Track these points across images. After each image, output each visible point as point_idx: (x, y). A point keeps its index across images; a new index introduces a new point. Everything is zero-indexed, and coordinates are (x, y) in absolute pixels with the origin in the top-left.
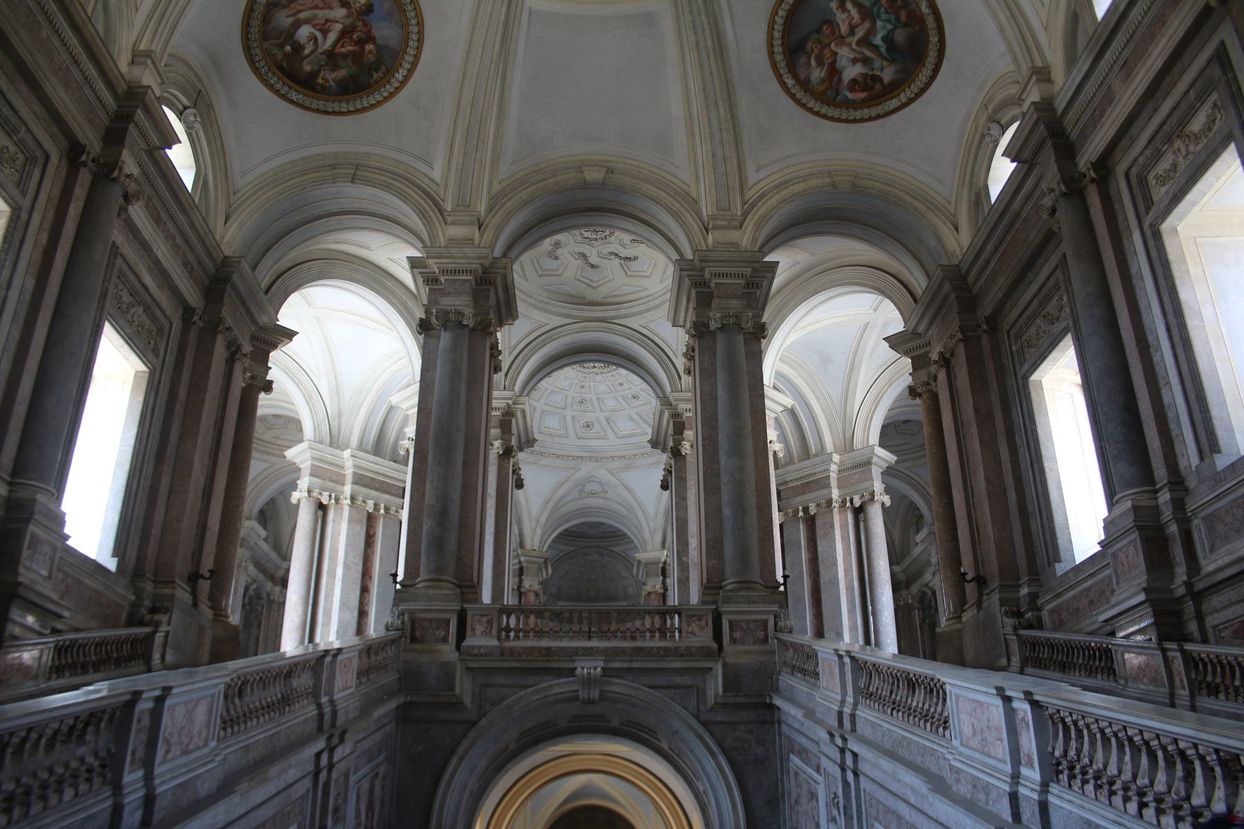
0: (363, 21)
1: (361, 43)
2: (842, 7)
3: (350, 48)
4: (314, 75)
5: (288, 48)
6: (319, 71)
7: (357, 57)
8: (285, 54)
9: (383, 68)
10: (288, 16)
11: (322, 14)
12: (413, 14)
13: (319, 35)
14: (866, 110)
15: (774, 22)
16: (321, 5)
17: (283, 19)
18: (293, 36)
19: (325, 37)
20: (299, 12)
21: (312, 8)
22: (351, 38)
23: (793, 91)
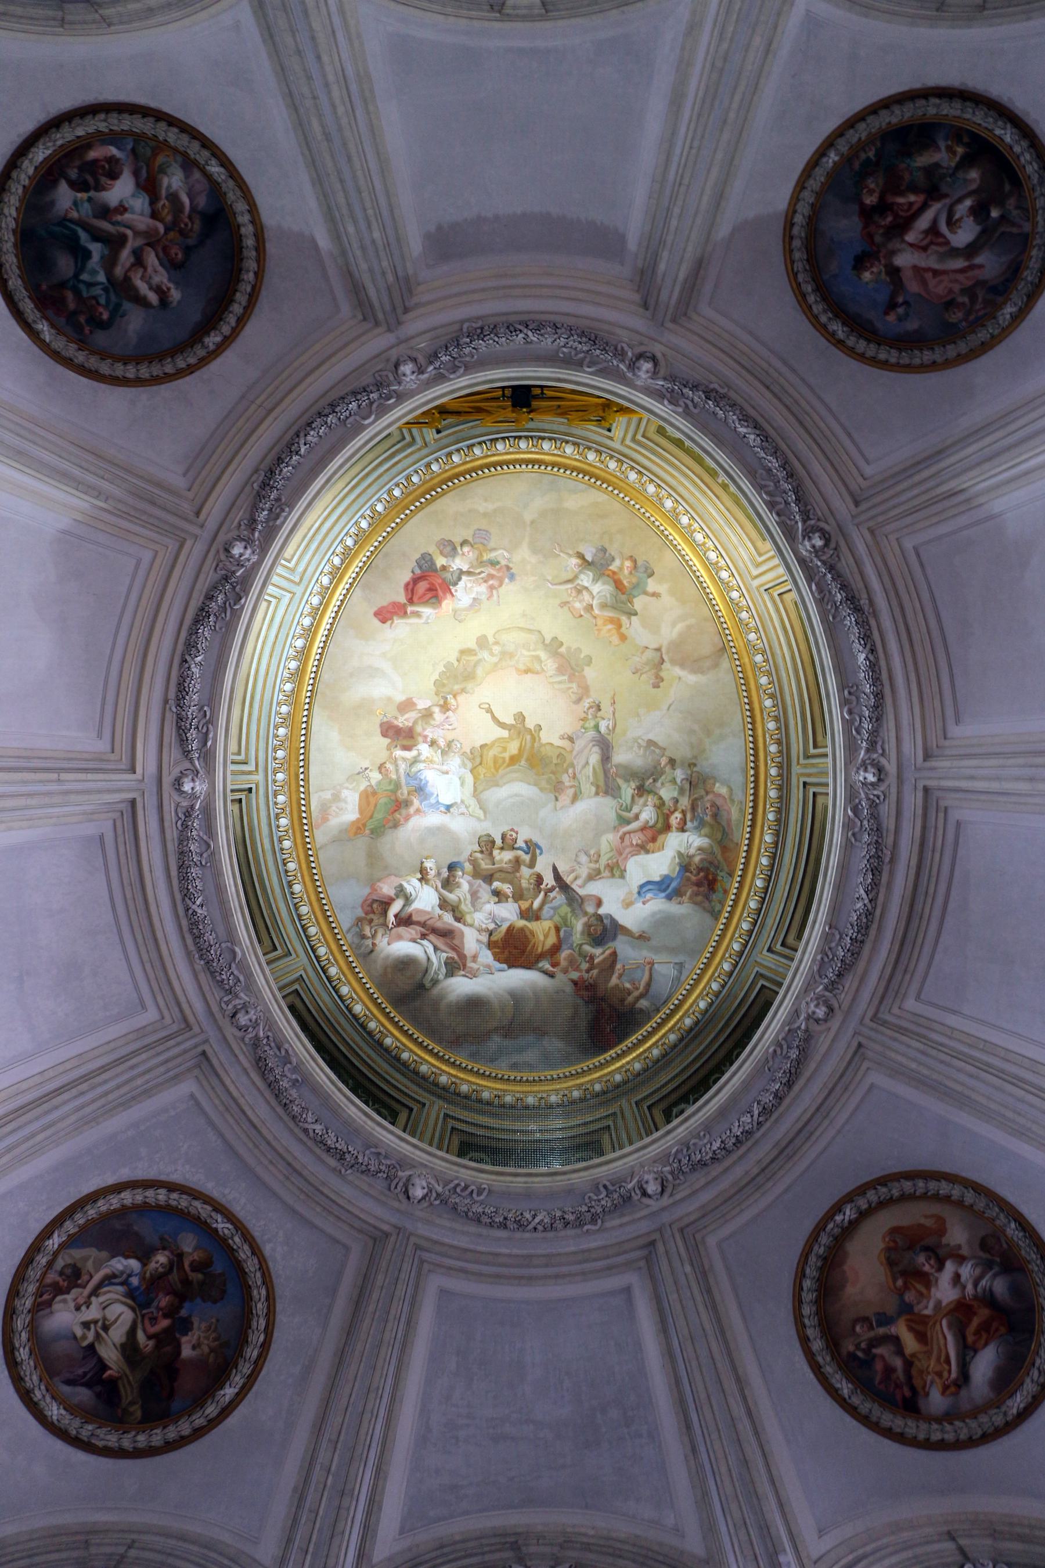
0: (873, 243)
1: (883, 207)
2: (162, 294)
3: (901, 200)
4: (967, 161)
5: (995, 214)
6: (958, 167)
7: (894, 185)
8: (1001, 204)
9: (857, 165)
10: (980, 267)
11: (929, 261)
12: (797, 255)
13: (943, 228)
14: (80, 132)
15: (258, 261)
16: (929, 276)
17: (990, 264)
18: (984, 231)
19: (935, 222)
20: (962, 271)
21: (944, 272)
22: (896, 216)
23: (206, 153)
